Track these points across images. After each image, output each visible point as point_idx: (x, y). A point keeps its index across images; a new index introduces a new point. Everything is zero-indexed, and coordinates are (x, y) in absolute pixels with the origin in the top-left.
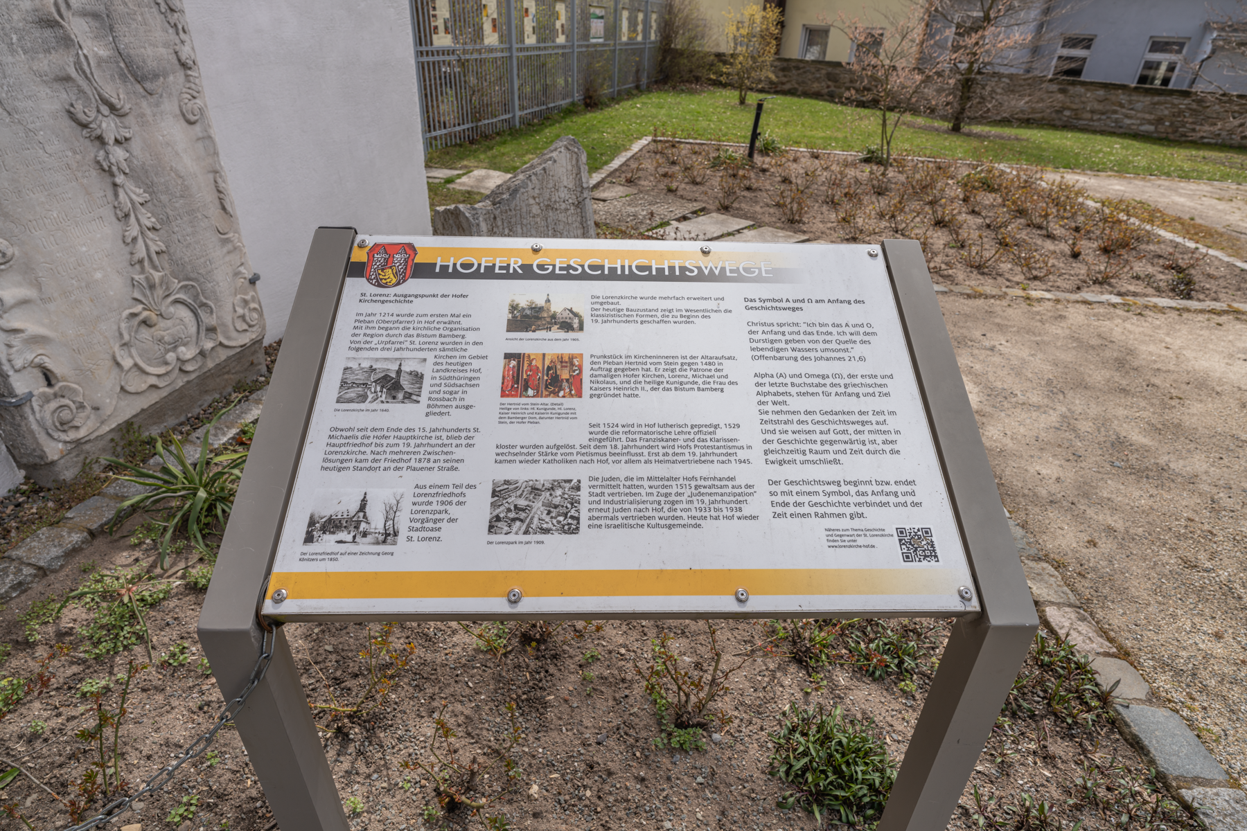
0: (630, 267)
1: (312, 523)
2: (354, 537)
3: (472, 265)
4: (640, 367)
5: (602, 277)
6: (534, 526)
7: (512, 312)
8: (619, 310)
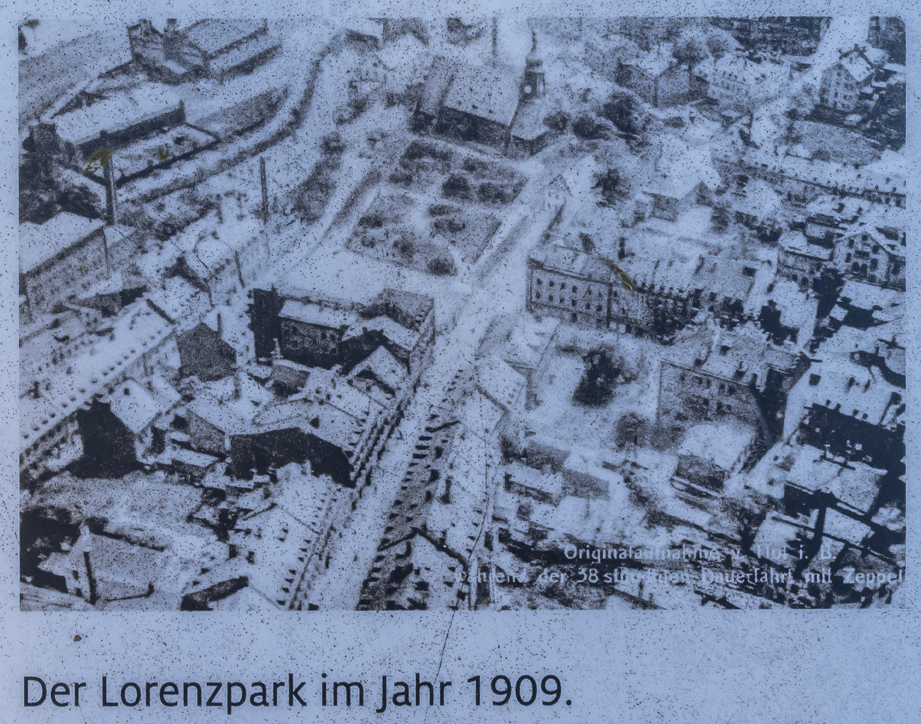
6: (456, 520)
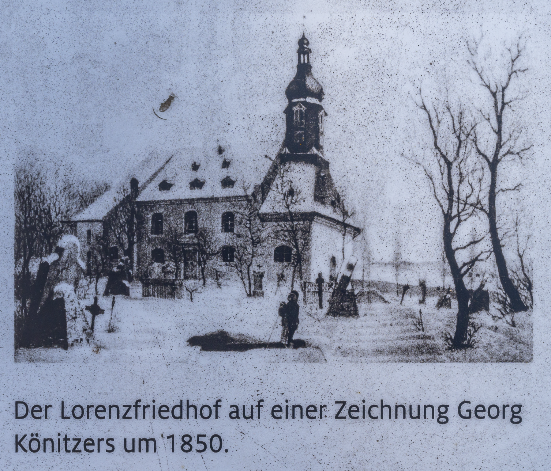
1: (36, 229)
2: (289, 313)
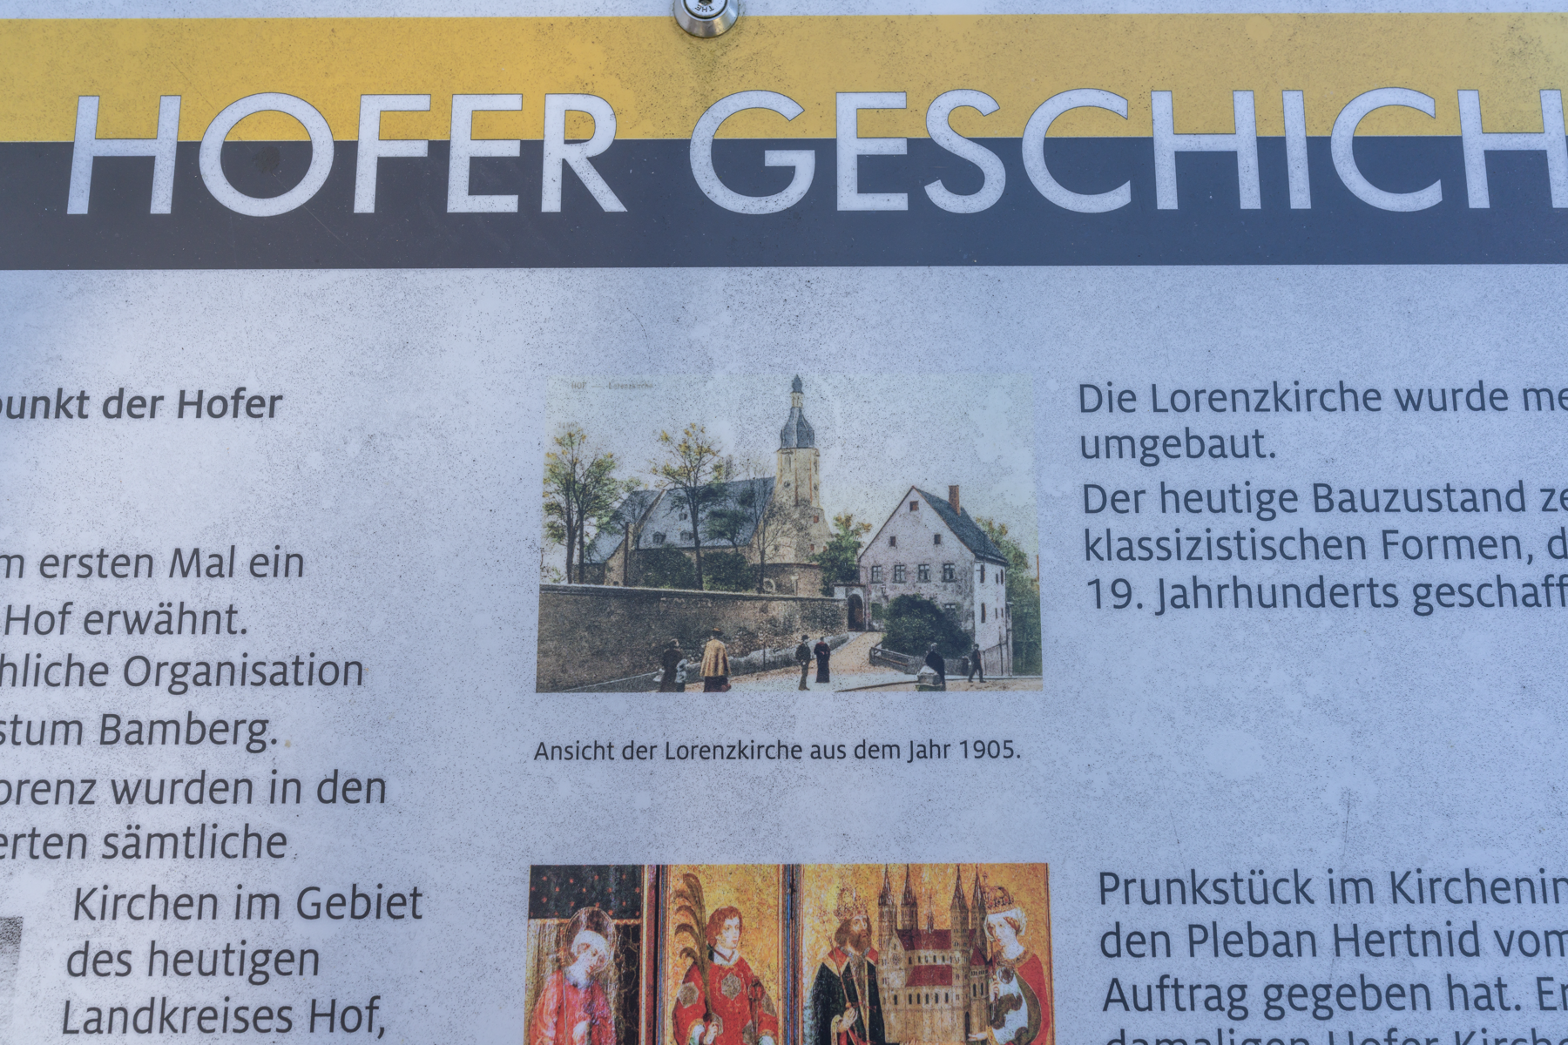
0: (1319, 148)
3: (294, 157)
4: (1431, 969)
5: (1136, 240)
7: (568, 533)
8: (1269, 503)
